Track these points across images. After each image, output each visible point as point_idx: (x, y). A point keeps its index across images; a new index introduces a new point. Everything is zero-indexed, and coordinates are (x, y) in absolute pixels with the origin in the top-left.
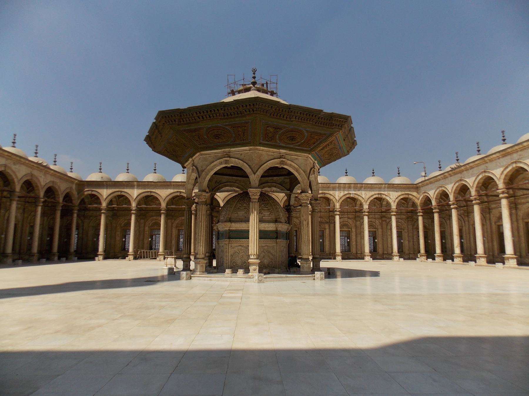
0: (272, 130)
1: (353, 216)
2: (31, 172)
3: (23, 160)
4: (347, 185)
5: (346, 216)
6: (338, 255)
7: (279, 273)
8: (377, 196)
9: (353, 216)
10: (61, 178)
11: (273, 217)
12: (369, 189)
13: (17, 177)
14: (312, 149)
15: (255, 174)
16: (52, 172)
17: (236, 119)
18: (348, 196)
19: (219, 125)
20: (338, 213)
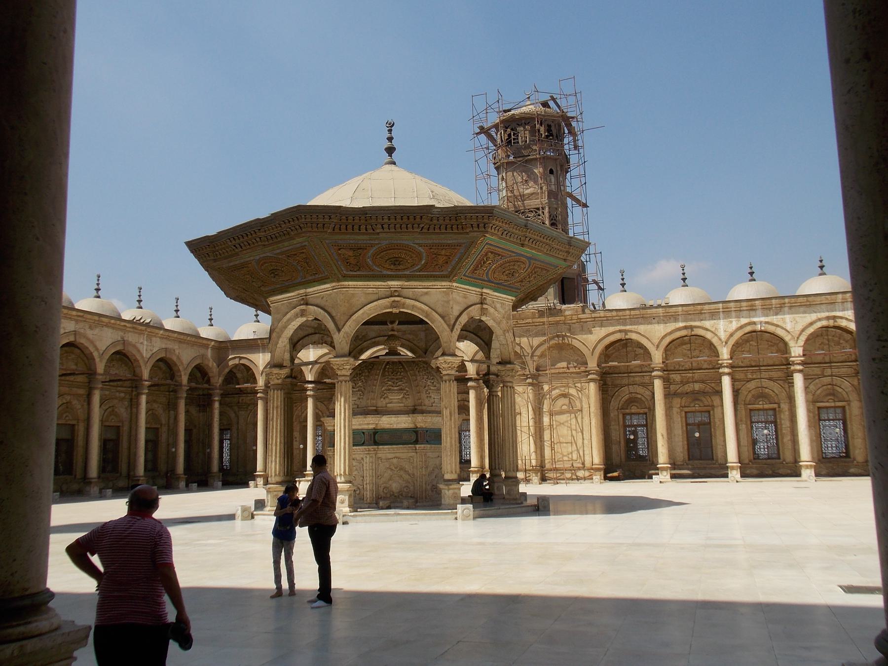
0: (351, 253)
1: (780, 374)
2: (122, 338)
3: (104, 319)
4: (744, 304)
5: (828, 372)
6: (733, 468)
7: (408, 508)
8: (824, 323)
9: (780, 374)
10: (181, 342)
11: (410, 402)
12: (802, 309)
13: (97, 349)
14: (451, 272)
15: (339, 330)
16: (161, 332)
17: (286, 244)
18: (749, 329)
19: (268, 254)
20: (727, 370)
